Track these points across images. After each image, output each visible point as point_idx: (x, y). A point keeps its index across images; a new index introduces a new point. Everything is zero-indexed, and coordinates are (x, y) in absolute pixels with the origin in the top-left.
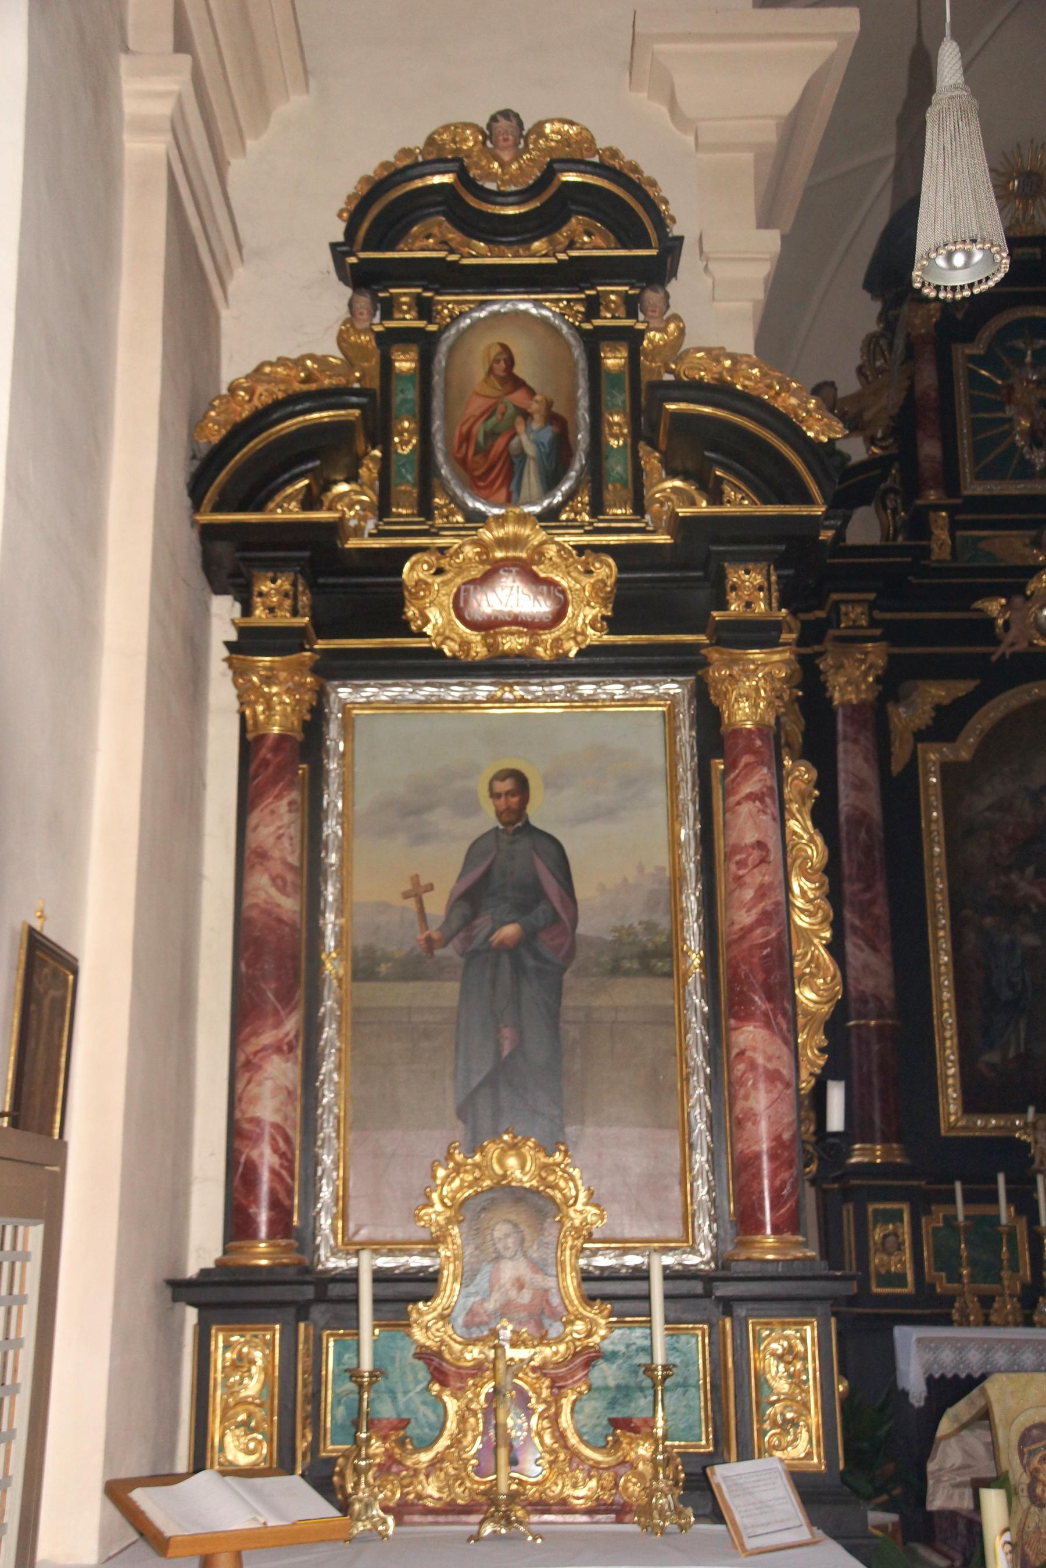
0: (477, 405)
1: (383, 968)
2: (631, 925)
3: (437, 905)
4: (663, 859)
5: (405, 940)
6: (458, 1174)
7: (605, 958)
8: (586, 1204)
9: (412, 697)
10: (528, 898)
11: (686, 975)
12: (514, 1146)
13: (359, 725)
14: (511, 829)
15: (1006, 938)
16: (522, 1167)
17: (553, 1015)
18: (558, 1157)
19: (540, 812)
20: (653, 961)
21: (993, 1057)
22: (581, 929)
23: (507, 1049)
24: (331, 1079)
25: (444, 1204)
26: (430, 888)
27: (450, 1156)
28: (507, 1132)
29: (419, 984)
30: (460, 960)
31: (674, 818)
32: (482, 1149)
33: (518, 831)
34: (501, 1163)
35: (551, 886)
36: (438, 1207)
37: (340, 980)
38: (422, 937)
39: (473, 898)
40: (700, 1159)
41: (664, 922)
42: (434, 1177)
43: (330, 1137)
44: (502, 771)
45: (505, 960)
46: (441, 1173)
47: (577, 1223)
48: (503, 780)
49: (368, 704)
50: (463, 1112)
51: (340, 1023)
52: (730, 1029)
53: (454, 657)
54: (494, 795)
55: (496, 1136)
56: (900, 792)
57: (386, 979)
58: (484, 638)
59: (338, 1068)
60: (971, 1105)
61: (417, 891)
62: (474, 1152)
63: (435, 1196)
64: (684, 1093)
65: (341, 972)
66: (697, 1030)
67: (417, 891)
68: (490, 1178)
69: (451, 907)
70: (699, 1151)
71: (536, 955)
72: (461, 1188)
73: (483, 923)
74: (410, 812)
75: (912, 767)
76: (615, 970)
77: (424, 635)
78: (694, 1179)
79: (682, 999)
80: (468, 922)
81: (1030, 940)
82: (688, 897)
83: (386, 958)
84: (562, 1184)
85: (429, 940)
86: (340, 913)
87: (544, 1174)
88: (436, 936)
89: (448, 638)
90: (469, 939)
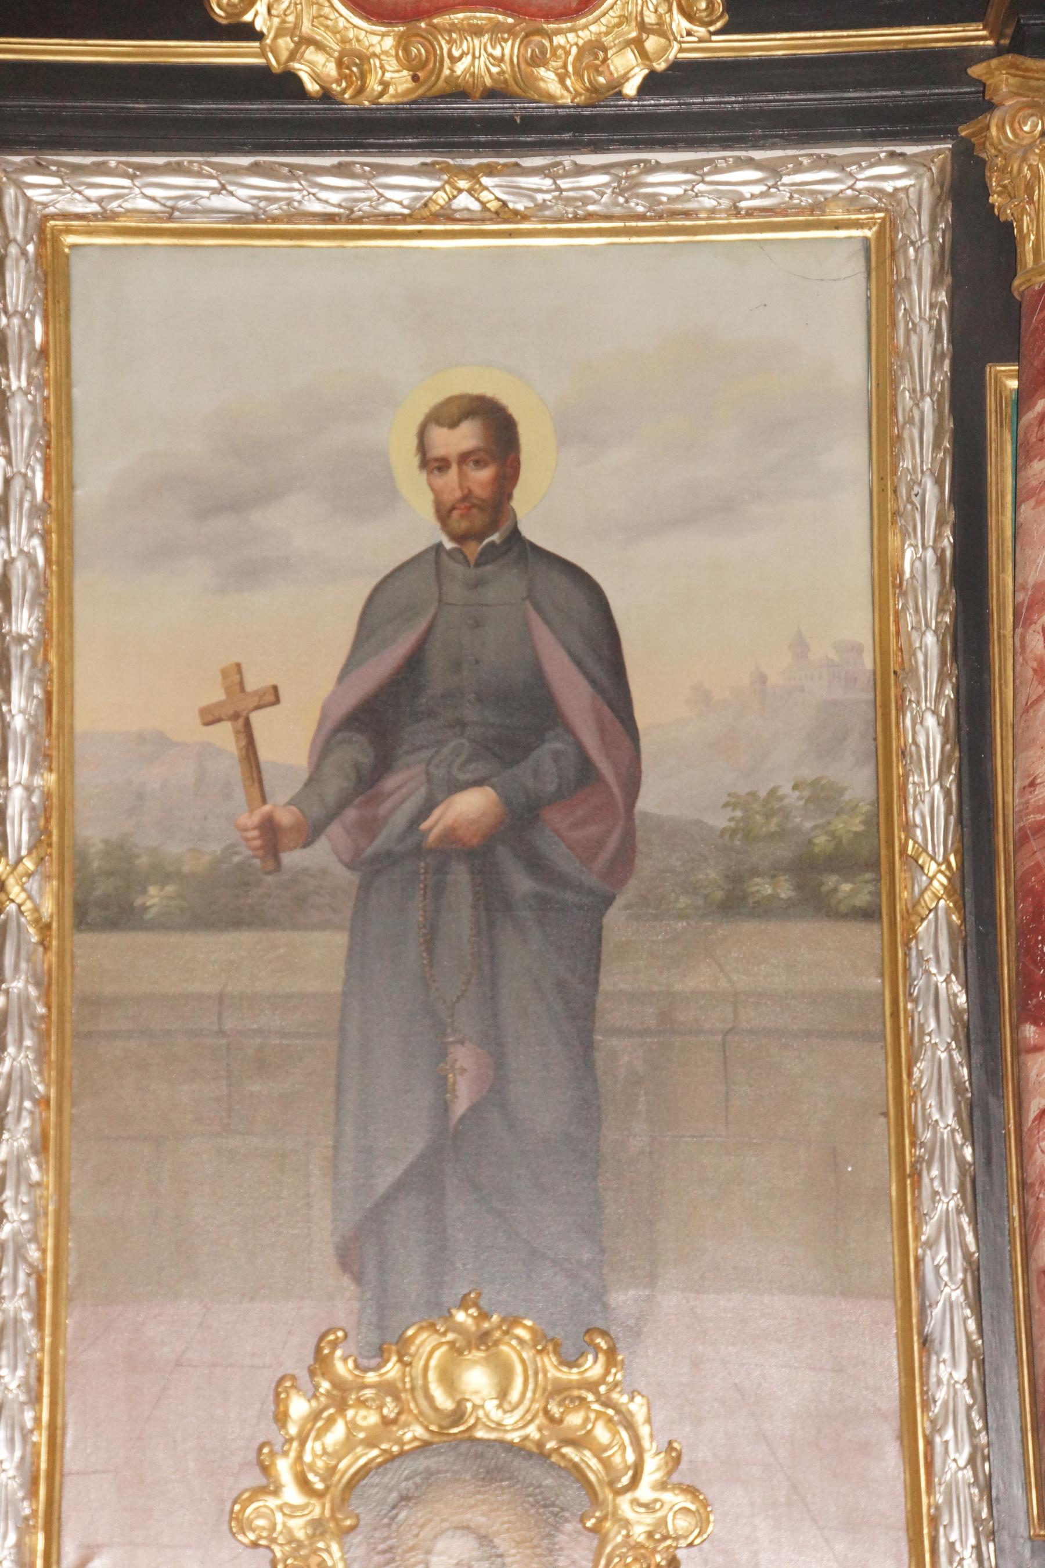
1: (154, 898)
2: (772, 792)
3: (289, 741)
4: (858, 625)
5: (211, 829)
6: (342, 1407)
7: (711, 874)
8: (662, 1486)
9: (219, 202)
10: (518, 722)
11: (914, 913)
12: (483, 1339)
13: (80, 272)
14: (473, 550)
16: (503, 1394)
17: (580, 1016)
18: (593, 1368)
20: (831, 880)
22: (647, 802)
23: (461, 1107)
24: (22, 1176)
25: (304, 1484)
26: (273, 696)
27: (321, 1363)
28: (464, 1304)
29: (246, 937)
30: (347, 878)
31: (886, 515)
32: (402, 1345)
33: (490, 554)
34: (449, 1381)
35: (575, 695)
36: (292, 1494)
37: (44, 928)
38: (256, 819)
40: (950, 1375)
41: (858, 784)
42: (281, 1418)
43: (17, 1321)
44: (449, 401)
45: (460, 875)
46: (299, 1407)
47: (639, 1533)
48: (453, 425)
49: (104, 219)
51: (43, 1037)
52: (1020, 1050)
53: (326, 96)
54: (432, 464)
55: (436, 1315)
57: (162, 925)
58: (403, 43)
59: (40, 1147)
61: (240, 707)
62: (381, 1353)
63: (283, 1467)
64: (904, 1217)
65: (48, 907)
66: (940, 1053)
68: (420, 1418)
69: (325, 748)
70: (946, 1355)
71: (536, 864)
72: (349, 1444)
73: (404, 784)
74: (220, 504)
76: (734, 903)
77: (248, 33)
78: (937, 1428)
79: (896, 971)
80: (368, 782)
82: (918, 720)
83: (164, 875)
84: (602, 1434)
85: (269, 828)
86: (40, 760)
87: (555, 1410)
88: (286, 817)
89: (310, 41)
90: (369, 827)
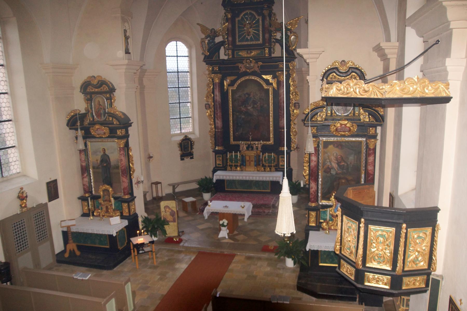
0: (97, 108)
3: (99, 162)
15: (240, 116)
19: (107, 152)
21: (237, 133)
39: (102, 161)
50: (103, 181)
56: (224, 95)
60: (234, 140)
61: (97, 160)
67: (97, 160)
74: (95, 153)
75: (228, 90)
81: (243, 117)
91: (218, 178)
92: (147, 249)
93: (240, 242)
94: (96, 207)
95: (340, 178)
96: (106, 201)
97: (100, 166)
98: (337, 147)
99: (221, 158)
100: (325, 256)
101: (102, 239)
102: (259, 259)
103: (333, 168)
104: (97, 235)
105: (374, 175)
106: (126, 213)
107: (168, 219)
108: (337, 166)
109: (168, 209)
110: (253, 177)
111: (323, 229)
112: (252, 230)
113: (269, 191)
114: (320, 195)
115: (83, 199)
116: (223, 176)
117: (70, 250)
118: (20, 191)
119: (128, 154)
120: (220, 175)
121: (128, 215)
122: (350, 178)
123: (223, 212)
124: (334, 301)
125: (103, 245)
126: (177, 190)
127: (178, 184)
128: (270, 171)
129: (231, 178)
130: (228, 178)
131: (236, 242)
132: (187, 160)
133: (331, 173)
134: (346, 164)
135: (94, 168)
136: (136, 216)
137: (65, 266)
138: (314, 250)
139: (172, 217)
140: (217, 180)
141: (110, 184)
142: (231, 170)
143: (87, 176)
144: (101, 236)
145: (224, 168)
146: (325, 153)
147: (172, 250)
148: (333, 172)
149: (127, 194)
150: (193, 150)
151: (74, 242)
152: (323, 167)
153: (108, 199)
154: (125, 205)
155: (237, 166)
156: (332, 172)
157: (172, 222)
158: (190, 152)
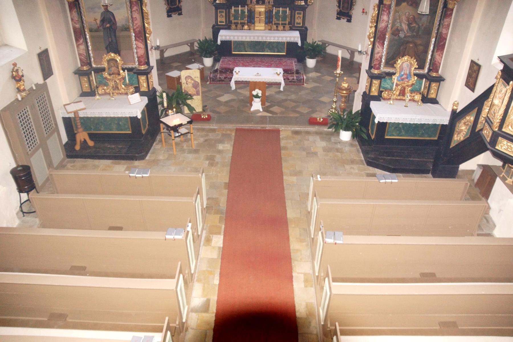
3: (98, 22)
4: (127, 15)
10: (110, 21)
19: (110, 9)
22: (118, 25)
35: (112, 19)
39: (103, 21)
50: (106, 48)
61: (95, 20)
67: (95, 20)
73: (104, 24)
76: (122, 30)
91: (224, 39)
92: (183, 130)
93: (279, 115)
94: (103, 83)
95: (408, 42)
96: (113, 74)
97: (101, 28)
98: (411, 5)
99: (224, 14)
100: (393, 128)
101: (120, 123)
102: (308, 133)
103: (402, 30)
104: (113, 119)
105: (446, 39)
106: (144, 87)
107: (190, 93)
108: (407, 27)
109: (189, 80)
110: (266, 37)
111: (384, 99)
112: (286, 100)
113: (284, 54)
114: (383, 61)
115: (79, 73)
116: (230, 36)
117: (81, 141)
118: (13, 69)
119: (142, 9)
120: (224, 35)
121: (147, 90)
122: (419, 42)
123: (255, 81)
124: (408, 174)
125: (122, 130)
126: (167, 54)
127: (167, 48)
128: (284, 30)
129: (240, 39)
130: (236, 39)
131: (274, 116)
132: (175, 16)
133: (399, 36)
134: (417, 26)
135: (91, 30)
136: (154, 90)
137: (79, 162)
138: (383, 122)
139: (195, 89)
140: (222, 42)
141: (117, 52)
142: (236, 29)
143: (83, 42)
144: (119, 119)
145: (228, 27)
146: (396, 11)
147: (203, 130)
148: (402, 35)
149: (144, 65)
150: (182, 4)
151: (84, 131)
152: (392, 28)
153: (116, 72)
154: (142, 78)
155: (245, 23)
156: (400, 35)
157: (195, 95)
158: (178, 7)
